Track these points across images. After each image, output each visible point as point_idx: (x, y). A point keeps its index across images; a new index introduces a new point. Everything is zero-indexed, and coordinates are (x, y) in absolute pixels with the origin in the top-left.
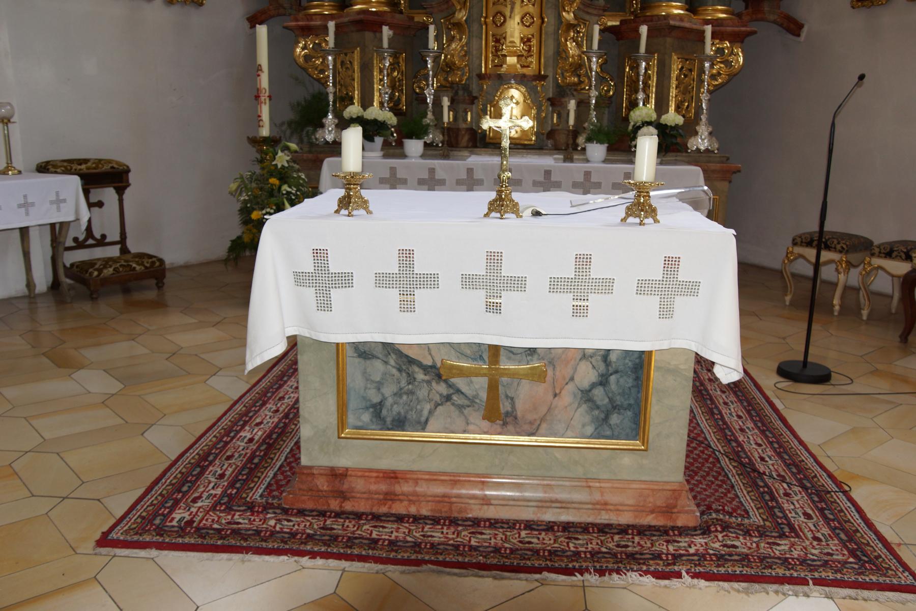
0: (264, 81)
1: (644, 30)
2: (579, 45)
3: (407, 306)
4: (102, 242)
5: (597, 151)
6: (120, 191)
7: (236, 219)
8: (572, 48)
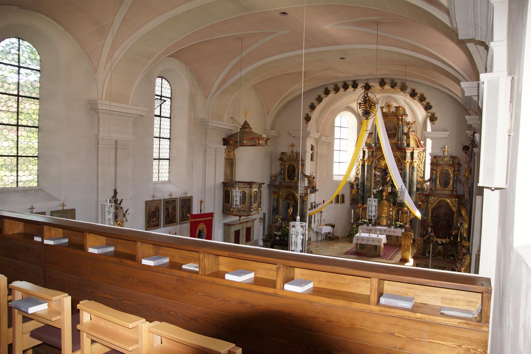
0: (353, 216)
1: (400, 212)
2: (392, 213)
3: (363, 241)
4: (331, 234)
5: (393, 227)
6: (333, 228)
7: (348, 232)
8: (391, 213)
